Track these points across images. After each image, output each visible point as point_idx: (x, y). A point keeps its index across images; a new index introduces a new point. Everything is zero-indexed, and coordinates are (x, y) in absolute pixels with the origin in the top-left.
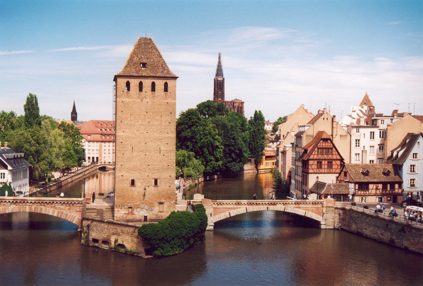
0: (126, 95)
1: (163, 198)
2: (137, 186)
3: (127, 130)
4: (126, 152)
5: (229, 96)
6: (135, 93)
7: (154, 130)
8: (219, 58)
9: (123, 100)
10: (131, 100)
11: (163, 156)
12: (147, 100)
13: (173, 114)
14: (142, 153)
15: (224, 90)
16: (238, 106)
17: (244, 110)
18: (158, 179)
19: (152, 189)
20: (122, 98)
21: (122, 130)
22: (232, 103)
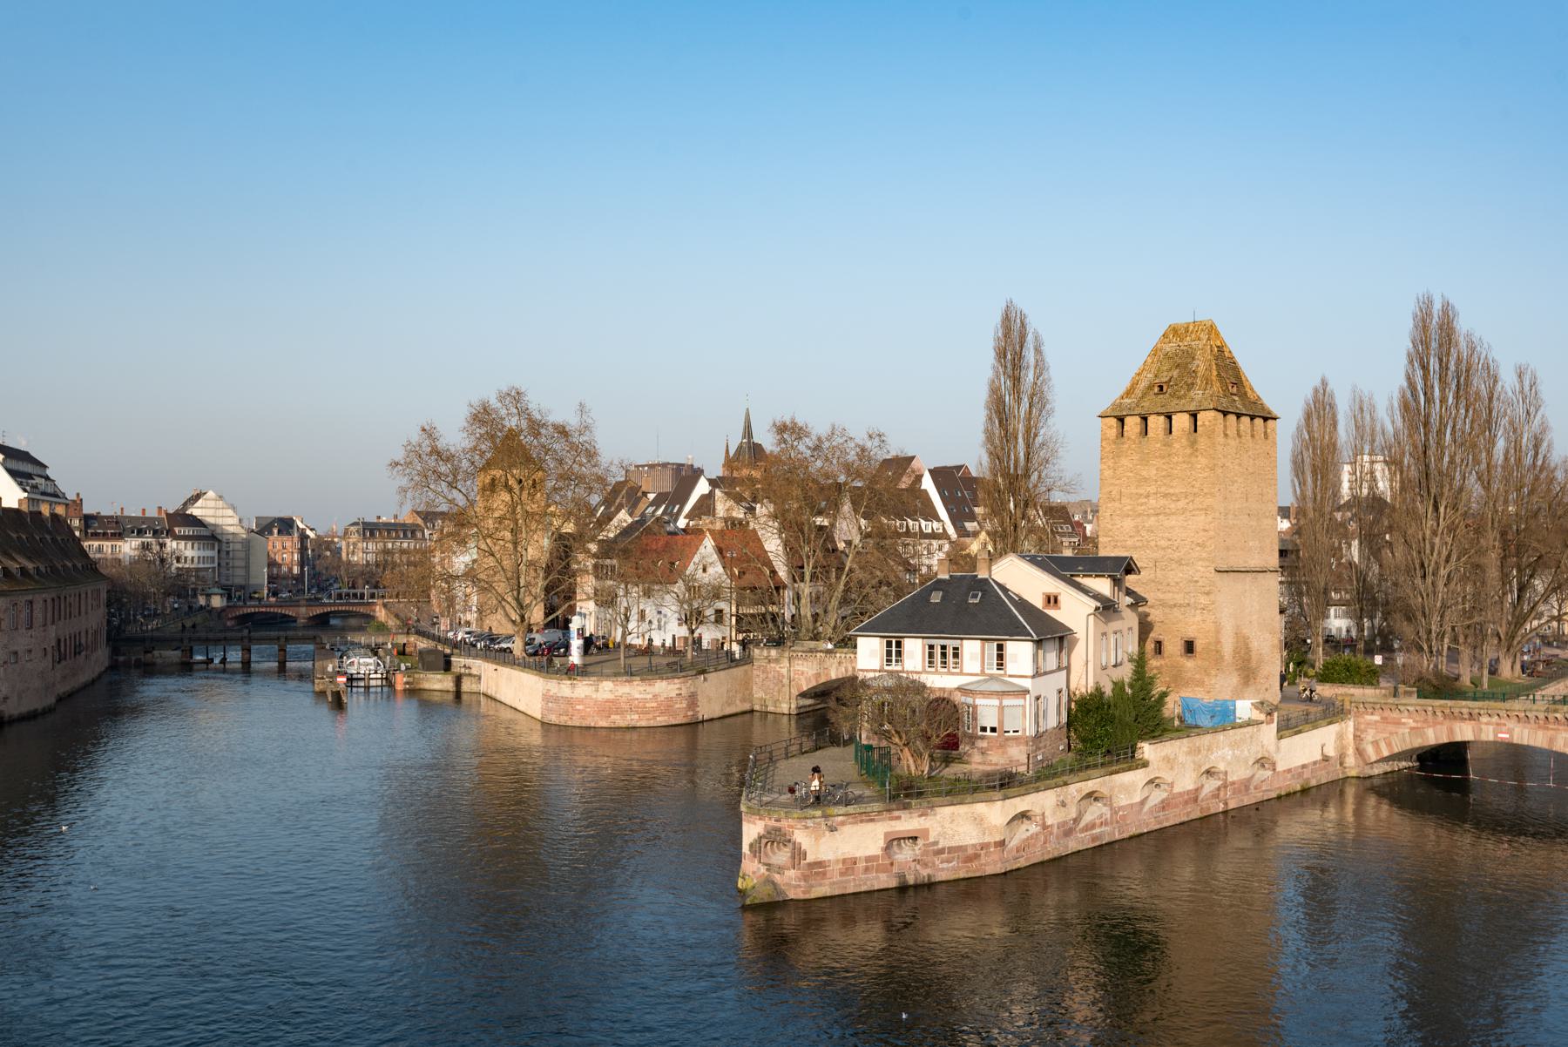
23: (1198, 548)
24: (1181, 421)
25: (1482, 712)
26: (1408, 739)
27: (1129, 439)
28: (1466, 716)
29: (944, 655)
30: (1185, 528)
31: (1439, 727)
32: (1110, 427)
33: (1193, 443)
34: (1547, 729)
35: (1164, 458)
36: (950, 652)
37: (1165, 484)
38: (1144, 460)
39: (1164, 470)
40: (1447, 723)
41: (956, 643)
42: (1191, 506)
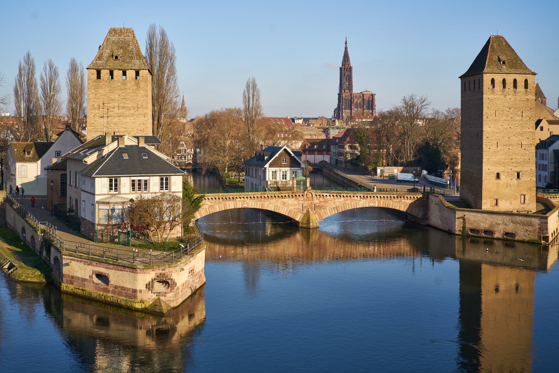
0: (491, 91)
1: (525, 191)
2: (501, 178)
3: (492, 126)
4: (492, 147)
5: (357, 89)
6: (499, 90)
7: (517, 125)
8: (346, 43)
9: (489, 97)
10: (496, 96)
11: (524, 150)
12: (510, 96)
13: (533, 109)
14: (505, 147)
15: (352, 80)
16: (369, 99)
17: (376, 103)
18: (521, 172)
19: (515, 181)
20: (487, 95)
21: (488, 125)
22: (362, 95)
23: (140, 132)
24: (131, 74)
25: (238, 197)
26: (208, 211)
27: (103, 80)
28: (231, 199)
29: (140, 185)
30: (134, 123)
31: (220, 204)
32: (93, 74)
33: (137, 84)
34: (261, 201)
35: (122, 90)
36: (143, 183)
37: (123, 103)
38: (112, 91)
39: (122, 96)
40: (224, 202)
41: (148, 178)
42: (137, 113)
